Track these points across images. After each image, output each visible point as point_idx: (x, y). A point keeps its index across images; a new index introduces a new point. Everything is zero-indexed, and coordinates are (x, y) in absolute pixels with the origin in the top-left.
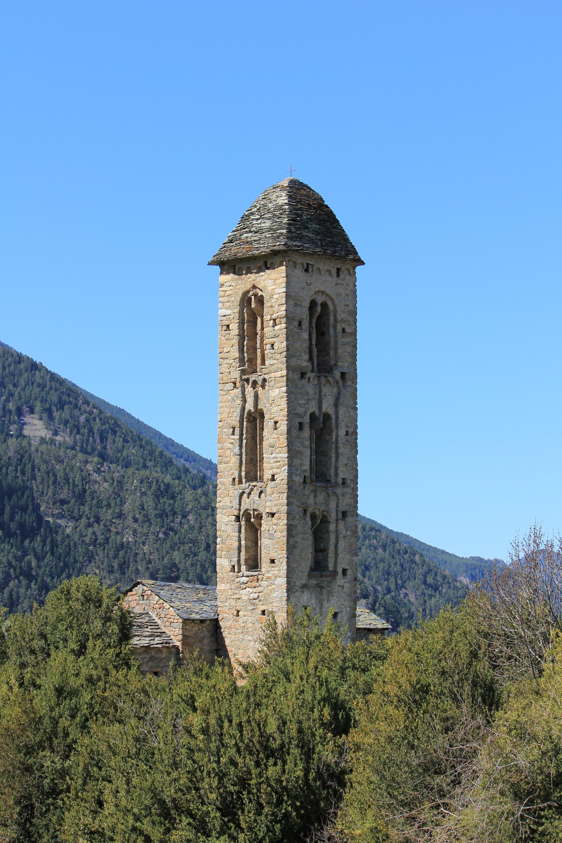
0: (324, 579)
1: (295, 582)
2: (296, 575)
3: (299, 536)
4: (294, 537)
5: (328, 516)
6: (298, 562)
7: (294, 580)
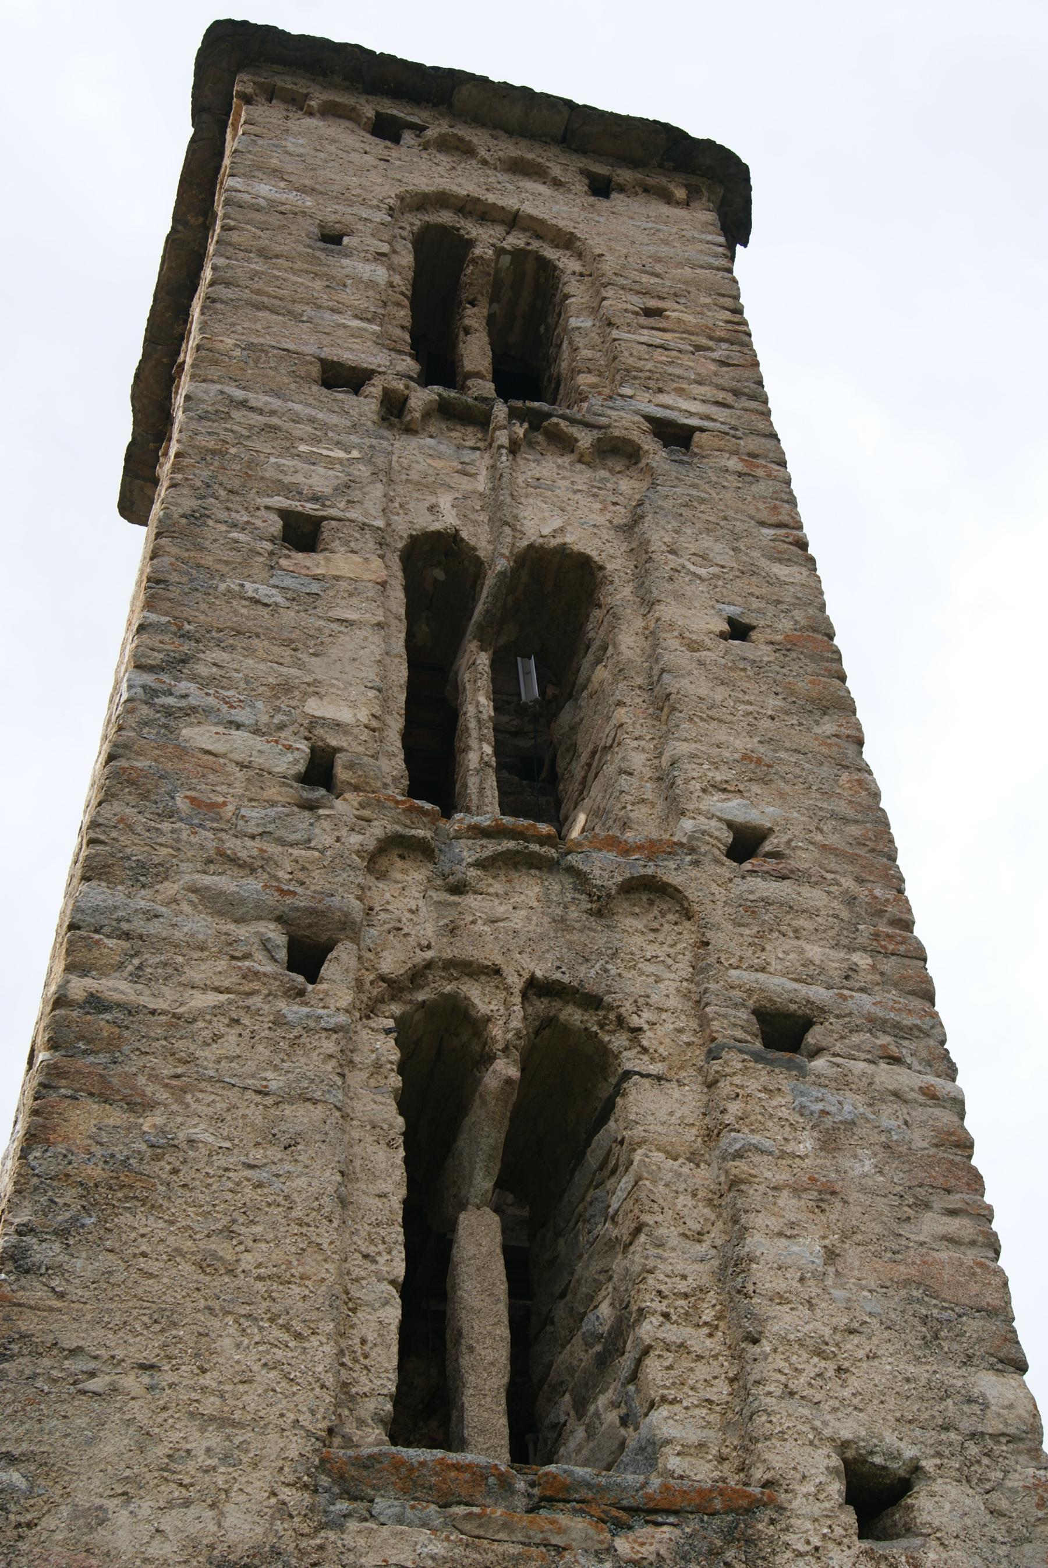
0: (576, 1527)
1: (100, 1518)
2: (114, 1443)
3: (207, 1101)
4: (138, 1105)
5: (618, 1041)
6: (165, 1319)
7: (89, 1489)
